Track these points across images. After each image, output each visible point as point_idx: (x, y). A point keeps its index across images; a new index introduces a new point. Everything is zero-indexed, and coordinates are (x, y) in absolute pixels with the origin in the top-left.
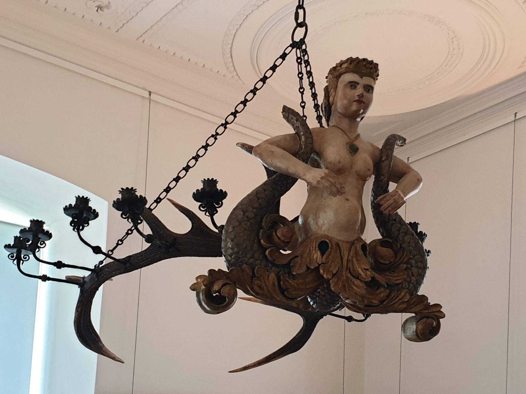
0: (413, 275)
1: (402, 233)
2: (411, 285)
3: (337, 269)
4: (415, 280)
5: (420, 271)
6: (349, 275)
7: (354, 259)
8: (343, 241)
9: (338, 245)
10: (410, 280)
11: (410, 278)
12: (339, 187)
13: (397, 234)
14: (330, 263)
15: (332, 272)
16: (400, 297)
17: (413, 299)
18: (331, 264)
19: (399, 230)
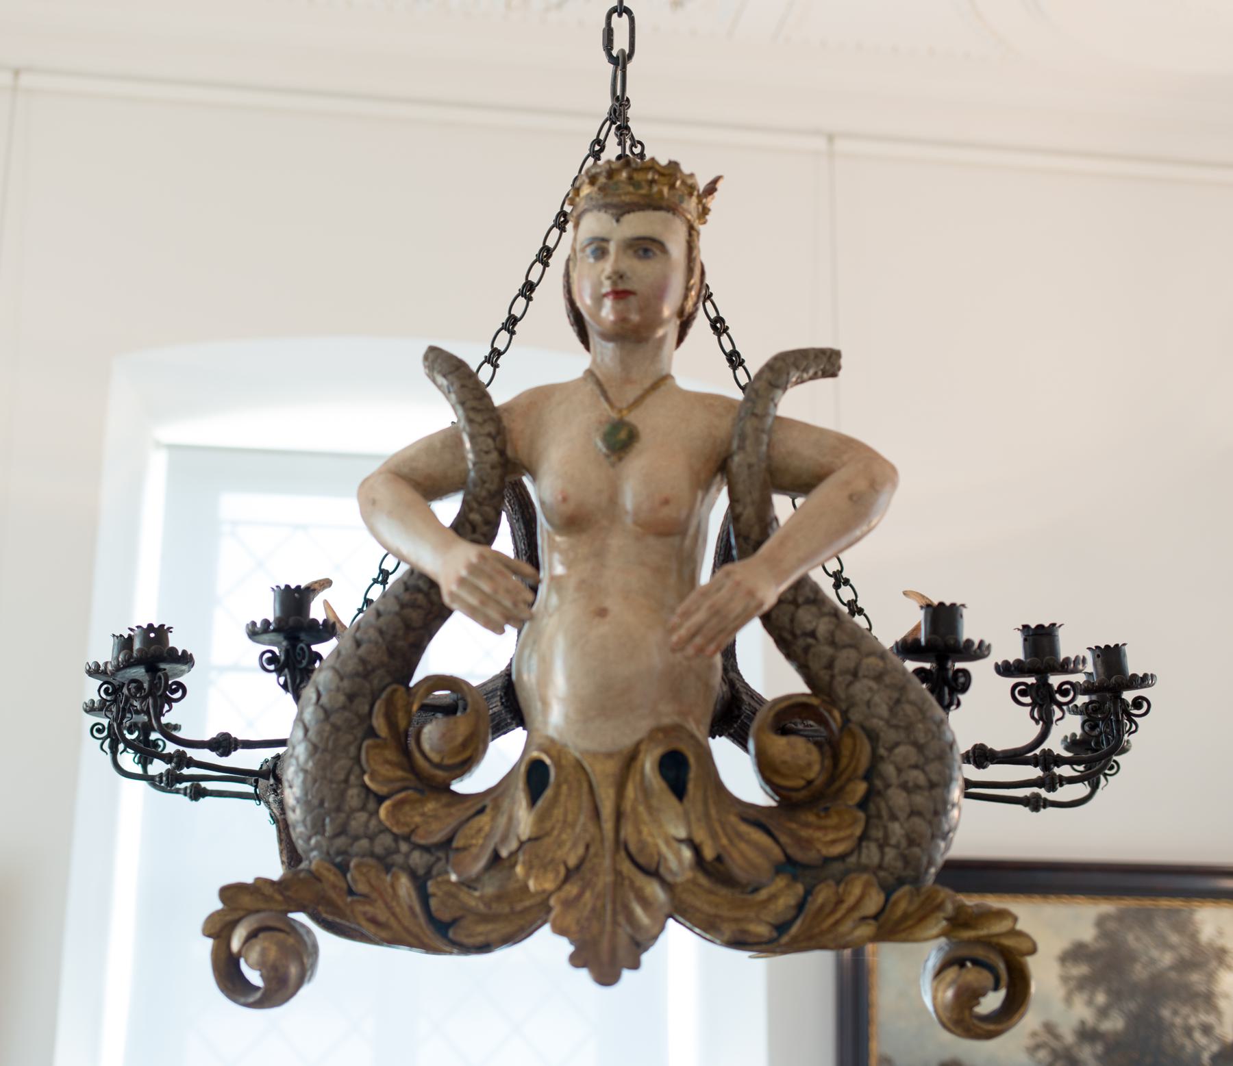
0: (894, 817)
1: (843, 673)
2: (890, 853)
3: (581, 850)
4: (902, 832)
5: (919, 799)
6: (626, 867)
7: (641, 809)
8: (595, 755)
9: (579, 765)
10: (886, 837)
11: (885, 828)
12: (508, 603)
13: (827, 678)
14: (555, 833)
15: (565, 864)
16: (851, 900)
17: (896, 903)
18: (559, 835)
19: (830, 666)
